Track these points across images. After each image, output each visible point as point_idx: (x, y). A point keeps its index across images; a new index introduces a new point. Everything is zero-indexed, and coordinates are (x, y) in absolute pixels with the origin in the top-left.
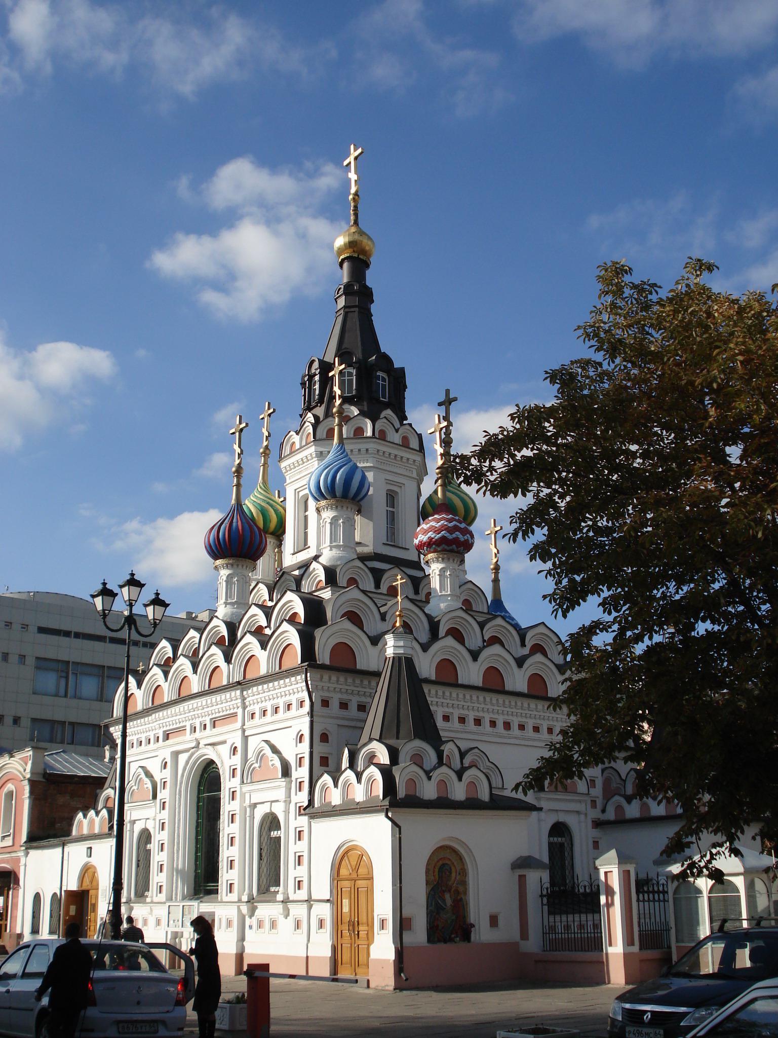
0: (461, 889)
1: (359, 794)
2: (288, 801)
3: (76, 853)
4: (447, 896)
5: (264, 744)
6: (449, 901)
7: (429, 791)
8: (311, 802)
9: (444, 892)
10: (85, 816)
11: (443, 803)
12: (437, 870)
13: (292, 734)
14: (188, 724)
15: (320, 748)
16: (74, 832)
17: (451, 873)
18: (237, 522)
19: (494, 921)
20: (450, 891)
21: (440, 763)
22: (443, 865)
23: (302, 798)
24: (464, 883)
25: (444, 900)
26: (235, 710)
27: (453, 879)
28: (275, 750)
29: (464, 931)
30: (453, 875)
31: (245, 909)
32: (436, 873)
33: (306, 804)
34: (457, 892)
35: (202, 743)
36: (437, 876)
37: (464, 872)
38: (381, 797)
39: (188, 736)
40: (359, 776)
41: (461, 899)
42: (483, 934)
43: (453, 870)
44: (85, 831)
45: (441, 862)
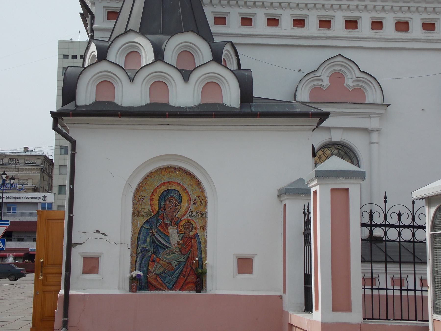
0: (196, 222)
4: (173, 232)
6: (174, 236)
9: (167, 225)
11: (158, 112)
12: (156, 197)
17: (180, 202)
19: (245, 265)
20: (177, 225)
22: (168, 191)
24: (203, 215)
29: (196, 278)
30: (185, 205)
34: (190, 226)
36: (156, 207)
37: (202, 200)
42: (222, 279)
45: (164, 188)
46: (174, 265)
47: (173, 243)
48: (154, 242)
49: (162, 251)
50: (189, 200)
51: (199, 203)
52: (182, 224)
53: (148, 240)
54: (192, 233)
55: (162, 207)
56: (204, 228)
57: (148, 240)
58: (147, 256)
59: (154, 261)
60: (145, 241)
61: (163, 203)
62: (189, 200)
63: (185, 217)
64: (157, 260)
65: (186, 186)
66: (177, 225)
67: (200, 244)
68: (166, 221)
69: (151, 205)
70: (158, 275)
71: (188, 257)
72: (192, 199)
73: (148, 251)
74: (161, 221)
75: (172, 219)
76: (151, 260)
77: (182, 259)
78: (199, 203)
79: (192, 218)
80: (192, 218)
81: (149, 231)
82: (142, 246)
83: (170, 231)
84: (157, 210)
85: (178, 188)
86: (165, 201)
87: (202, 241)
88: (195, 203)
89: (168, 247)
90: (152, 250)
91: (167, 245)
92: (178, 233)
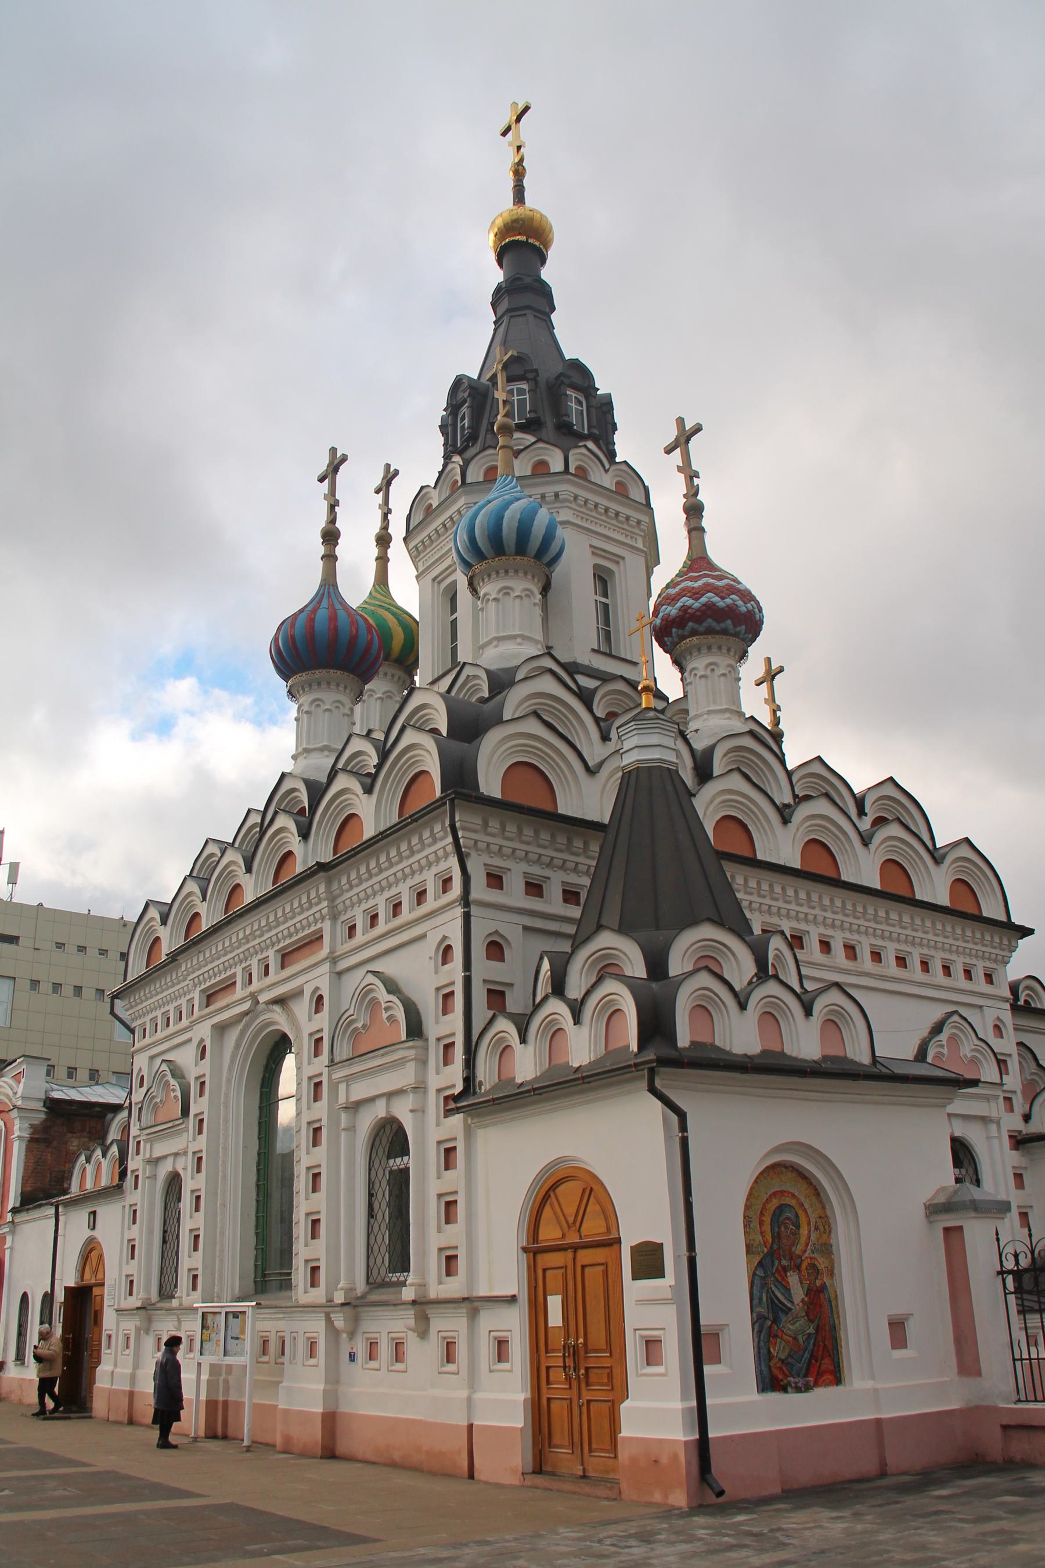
0: (822, 1263)
1: (581, 1048)
2: (420, 1088)
3: (75, 1227)
4: (793, 1279)
5: (371, 979)
7: (741, 1035)
8: (469, 1080)
9: (785, 1269)
10: (88, 1160)
11: (773, 1068)
12: (767, 1219)
13: (430, 947)
14: (238, 970)
15: (484, 968)
16: (75, 1189)
17: (798, 1227)
18: (323, 614)
20: (798, 1268)
21: (763, 972)
22: (781, 1208)
23: (454, 1076)
24: (827, 1249)
25: (787, 1289)
26: (319, 925)
27: (803, 1240)
28: (392, 987)
30: (804, 1231)
31: (339, 1322)
32: (767, 1227)
33: (459, 1088)
35: (263, 998)
37: (825, 1224)
38: (634, 1047)
39: (239, 992)
40: (577, 1011)
41: (824, 1287)
43: (803, 1220)
44: (89, 1185)
45: (775, 1203)
46: (801, 1341)
47: (796, 1302)
48: (772, 1301)
49: (783, 1318)
50: (809, 1224)
51: (822, 1228)
52: (804, 1267)
53: (764, 1299)
54: (818, 1283)
55: (777, 1237)
56: (831, 1274)
57: (764, 1299)
58: (766, 1326)
59: (776, 1336)
60: (760, 1299)
61: (777, 1229)
62: (809, 1224)
63: (807, 1255)
64: (779, 1333)
65: (802, 1199)
66: (798, 1268)
67: (830, 1301)
68: (784, 1262)
69: (761, 1233)
70: (782, 1361)
71: (818, 1326)
72: (813, 1221)
73: (766, 1318)
74: (777, 1262)
75: (791, 1259)
76: (772, 1335)
77: (811, 1330)
78: (822, 1228)
79: (816, 1255)
80: (816, 1255)
81: (764, 1285)
82: (758, 1309)
83: (790, 1280)
84: (770, 1241)
85: (793, 1203)
86: (779, 1227)
87: (832, 1296)
88: (816, 1229)
89: (790, 1309)
90: (771, 1316)
91: (789, 1305)
92: (801, 1283)
